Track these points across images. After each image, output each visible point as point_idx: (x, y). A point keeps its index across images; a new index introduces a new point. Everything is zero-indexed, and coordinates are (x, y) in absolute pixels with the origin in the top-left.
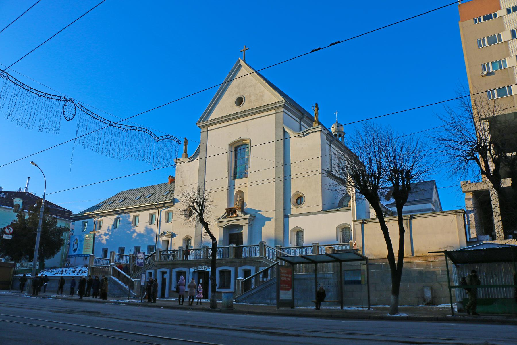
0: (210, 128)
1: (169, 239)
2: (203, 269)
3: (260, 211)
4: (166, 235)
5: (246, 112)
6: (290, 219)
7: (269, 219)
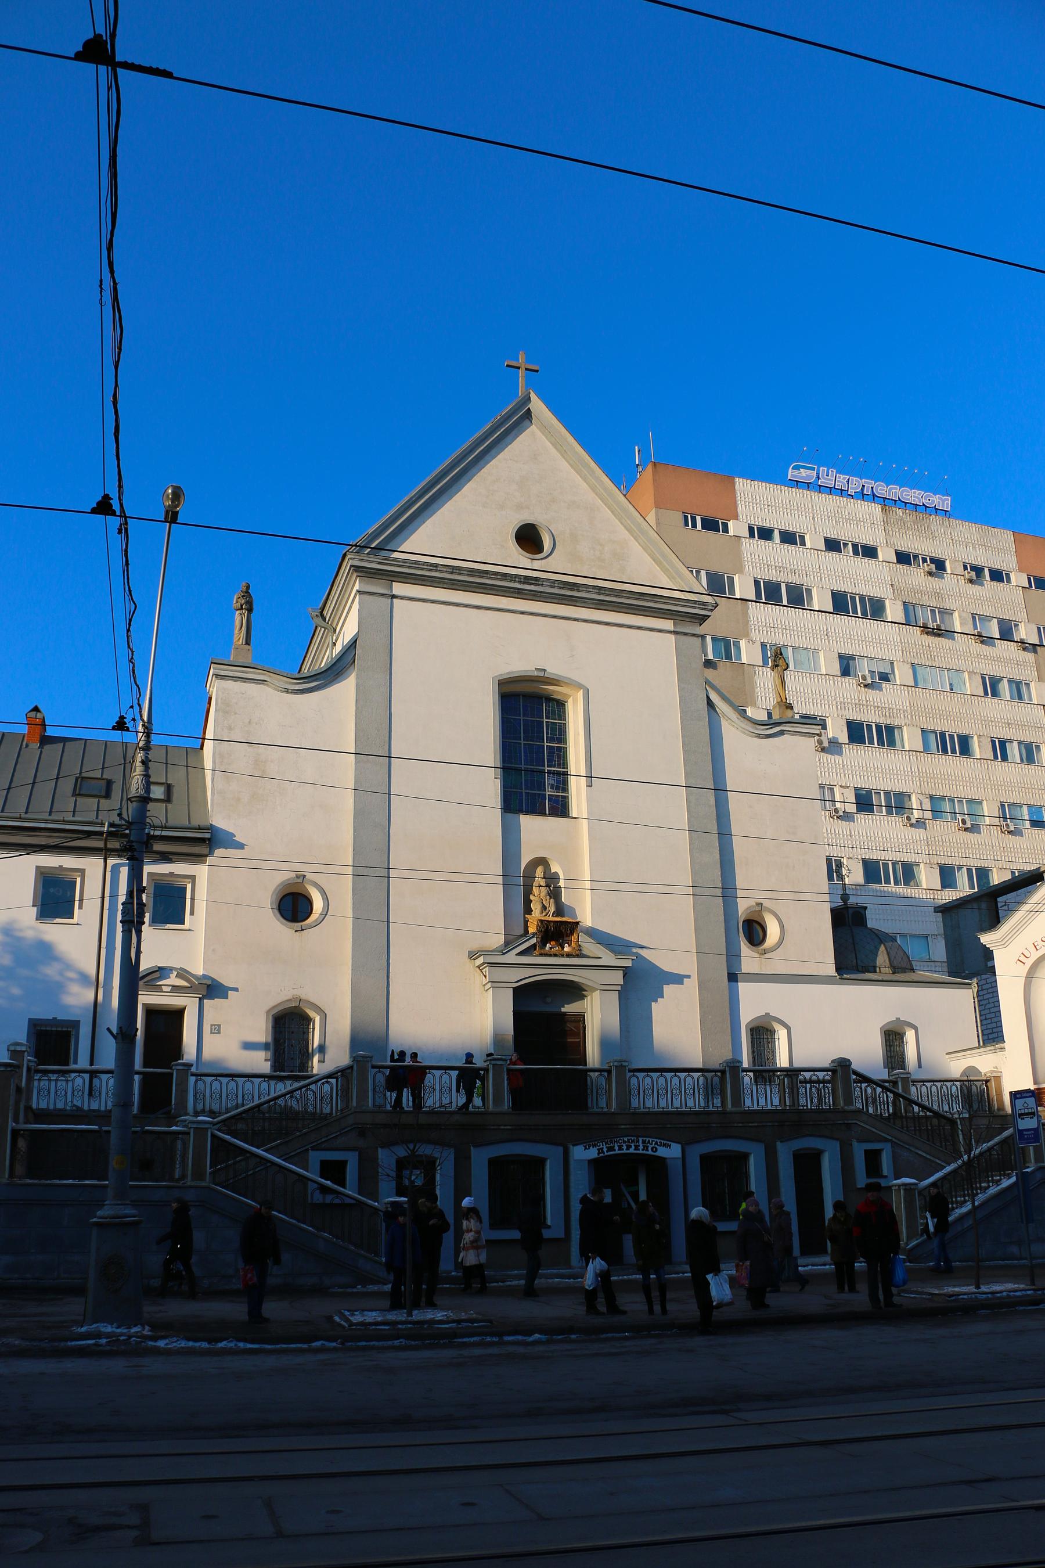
0: (398, 588)
1: (190, 1004)
2: (641, 1147)
3: (642, 947)
4: (173, 980)
5: (572, 590)
6: (743, 987)
7: (678, 979)
